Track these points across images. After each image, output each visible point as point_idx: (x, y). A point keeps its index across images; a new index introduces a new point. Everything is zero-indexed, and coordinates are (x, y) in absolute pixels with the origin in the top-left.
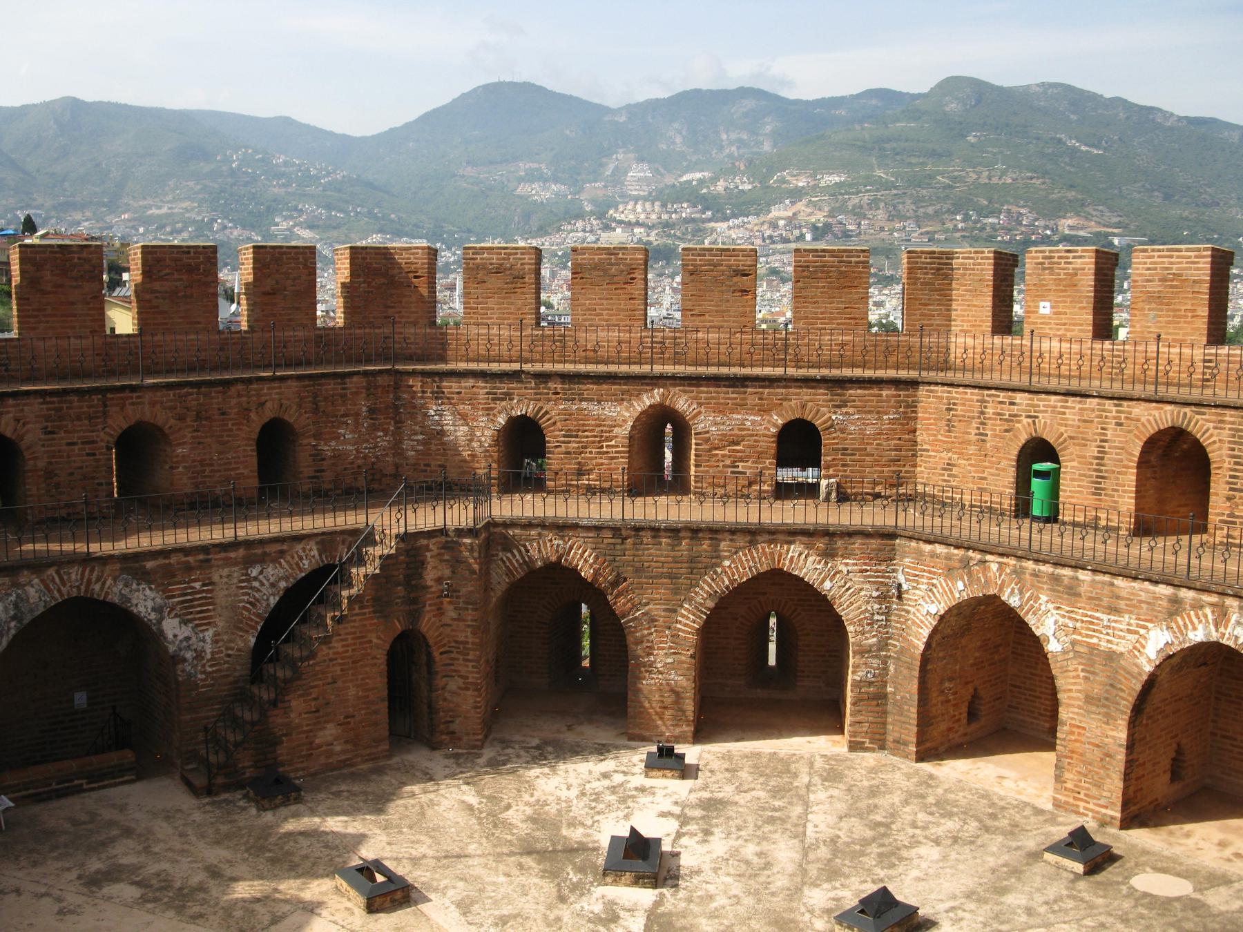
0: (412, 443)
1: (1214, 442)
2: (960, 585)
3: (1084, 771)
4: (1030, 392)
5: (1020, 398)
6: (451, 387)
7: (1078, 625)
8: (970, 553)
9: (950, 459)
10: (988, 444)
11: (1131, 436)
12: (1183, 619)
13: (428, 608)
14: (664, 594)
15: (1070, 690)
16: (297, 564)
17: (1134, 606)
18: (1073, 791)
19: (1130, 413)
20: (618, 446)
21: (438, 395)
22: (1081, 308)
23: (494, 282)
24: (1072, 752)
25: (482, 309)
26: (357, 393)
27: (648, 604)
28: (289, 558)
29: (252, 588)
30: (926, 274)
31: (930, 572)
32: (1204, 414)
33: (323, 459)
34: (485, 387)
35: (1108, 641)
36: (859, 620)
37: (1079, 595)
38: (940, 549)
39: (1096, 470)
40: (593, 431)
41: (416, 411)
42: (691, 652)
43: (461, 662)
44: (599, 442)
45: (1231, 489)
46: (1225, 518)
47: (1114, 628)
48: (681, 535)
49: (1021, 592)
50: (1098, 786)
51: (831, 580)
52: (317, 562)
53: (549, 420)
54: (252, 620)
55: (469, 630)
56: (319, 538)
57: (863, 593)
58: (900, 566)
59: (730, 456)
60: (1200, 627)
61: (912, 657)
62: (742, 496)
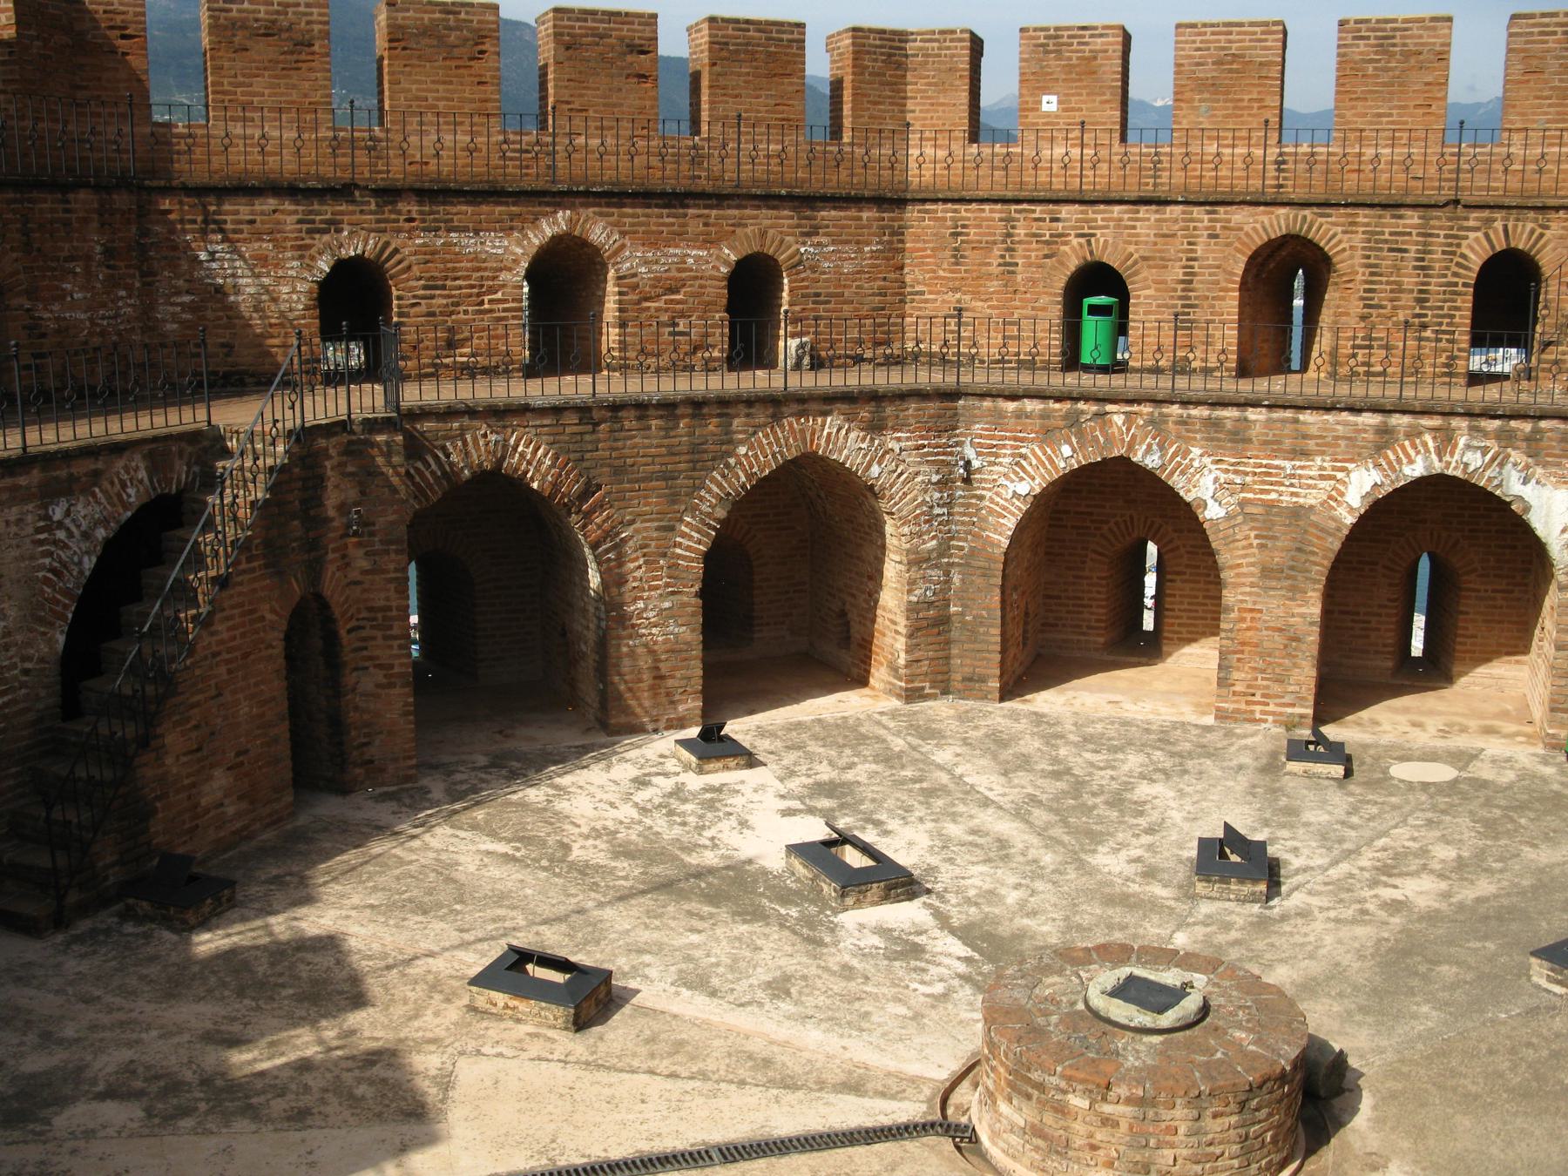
0: (171, 309)
1: (1344, 250)
2: (1066, 450)
3: (1261, 665)
4: (1082, 202)
5: (1065, 211)
6: (237, 213)
7: (1248, 479)
8: (1081, 405)
9: (959, 301)
10: (1019, 277)
11: (1230, 250)
12: (1395, 453)
13: (331, 556)
14: (657, 504)
15: (1239, 565)
16: (119, 496)
17: (1326, 445)
18: (1245, 694)
19: (1229, 221)
20: (506, 301)
21: (211, 225)
22: (1103, 102)
23: (263, 50)
24: (1243, 644)
25: (243, 94)
26: (85, 221)
27: (632, 522)
28: (106, 485)
29: (56, 542)
30: (875, 60)
31: (1015, 439)
32: (1329, 216)
33: (44, 335)
34: (296, 212)
35: (1293, 494)
36: (916, 517)
37: (1249, 441)
38: (1030, 405)
39: (1181, 298)
40: (468, 278)
41: (178, 254)
42: (697, 588)
43: (380, 641)
44: (478, 295)
45: (1366, 306)
47: (1301, 476)
48: (679, 411)
49: (1161, 447)
50: (1280, 680)
51: (880, 463)
52: (147, 491)
53: (400, 262)
54: (58, 602)
55: (392, 586)
56: (147, 447)
57: (919, 479)
58: (966, 436)
59: (666, 310)
60: (1419, 459)
61: (990, 559)
62: (685, 369)
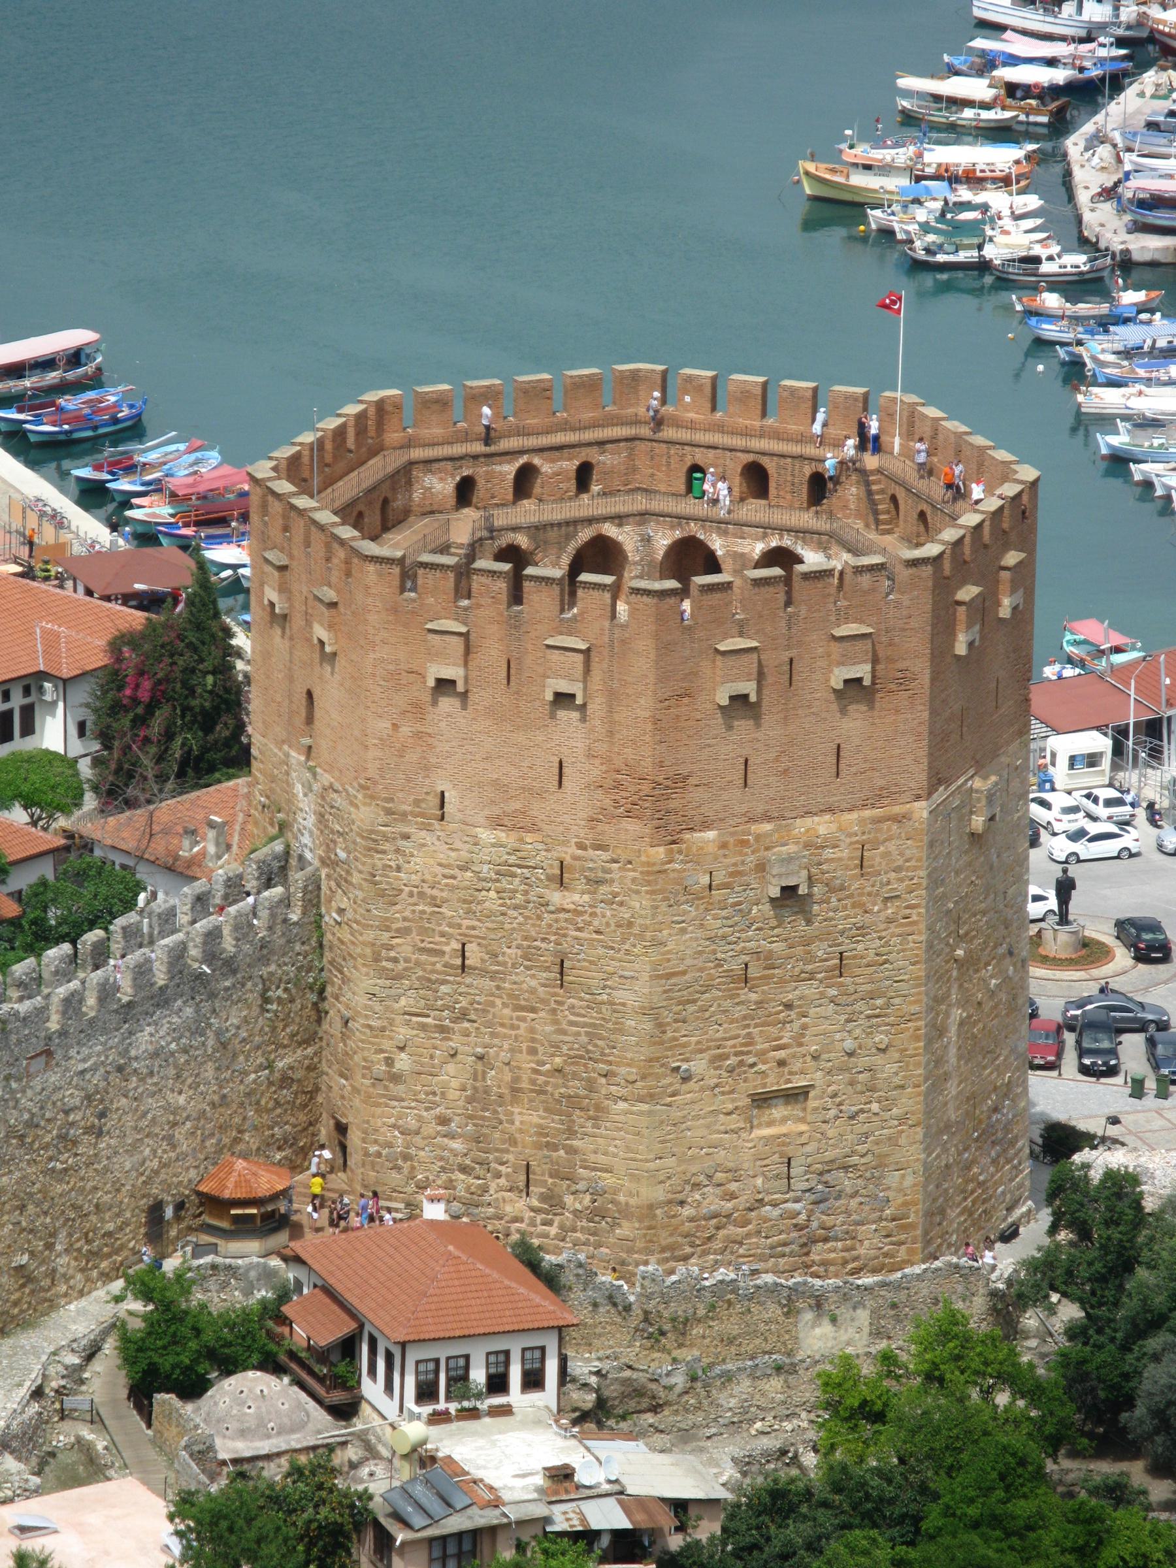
17: (750, 536)
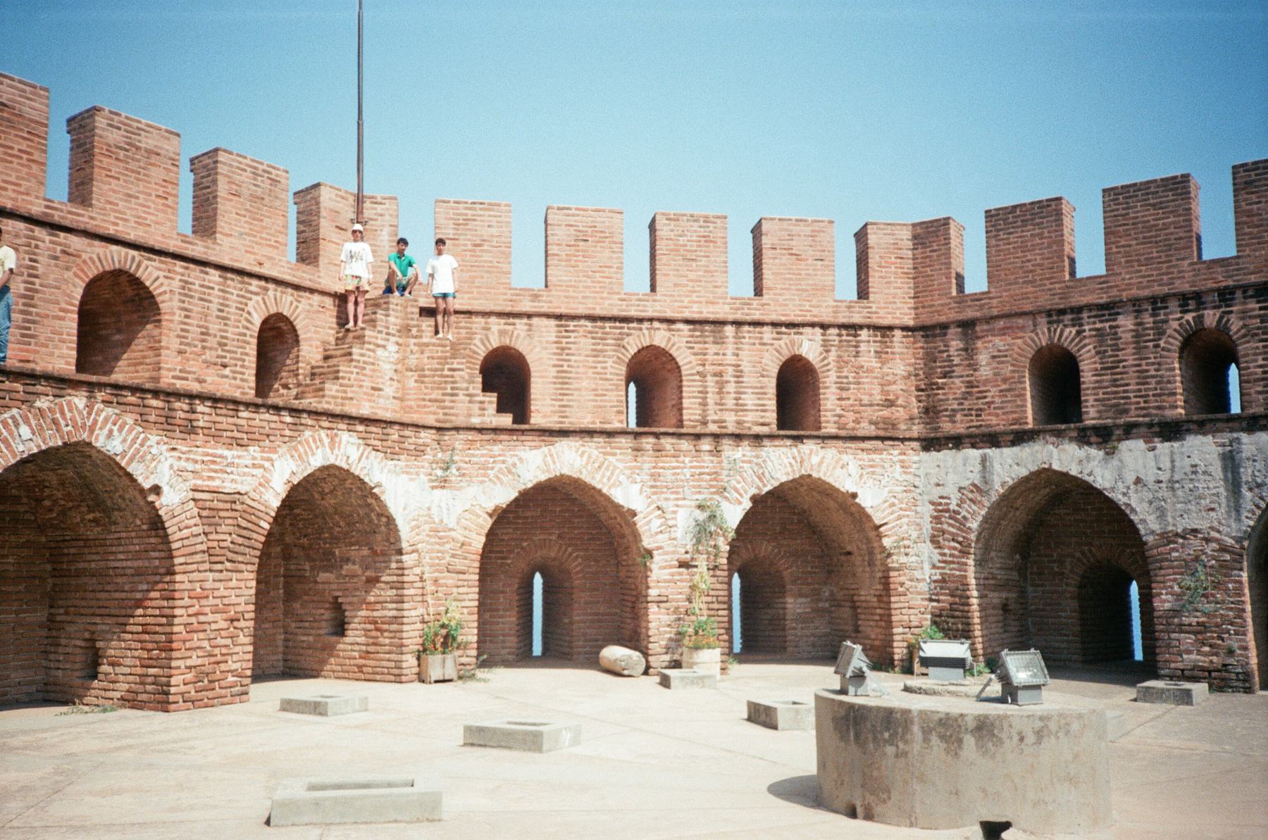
1: (165, 292)
46: (177, 373)
